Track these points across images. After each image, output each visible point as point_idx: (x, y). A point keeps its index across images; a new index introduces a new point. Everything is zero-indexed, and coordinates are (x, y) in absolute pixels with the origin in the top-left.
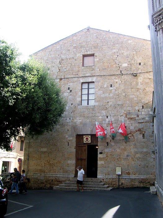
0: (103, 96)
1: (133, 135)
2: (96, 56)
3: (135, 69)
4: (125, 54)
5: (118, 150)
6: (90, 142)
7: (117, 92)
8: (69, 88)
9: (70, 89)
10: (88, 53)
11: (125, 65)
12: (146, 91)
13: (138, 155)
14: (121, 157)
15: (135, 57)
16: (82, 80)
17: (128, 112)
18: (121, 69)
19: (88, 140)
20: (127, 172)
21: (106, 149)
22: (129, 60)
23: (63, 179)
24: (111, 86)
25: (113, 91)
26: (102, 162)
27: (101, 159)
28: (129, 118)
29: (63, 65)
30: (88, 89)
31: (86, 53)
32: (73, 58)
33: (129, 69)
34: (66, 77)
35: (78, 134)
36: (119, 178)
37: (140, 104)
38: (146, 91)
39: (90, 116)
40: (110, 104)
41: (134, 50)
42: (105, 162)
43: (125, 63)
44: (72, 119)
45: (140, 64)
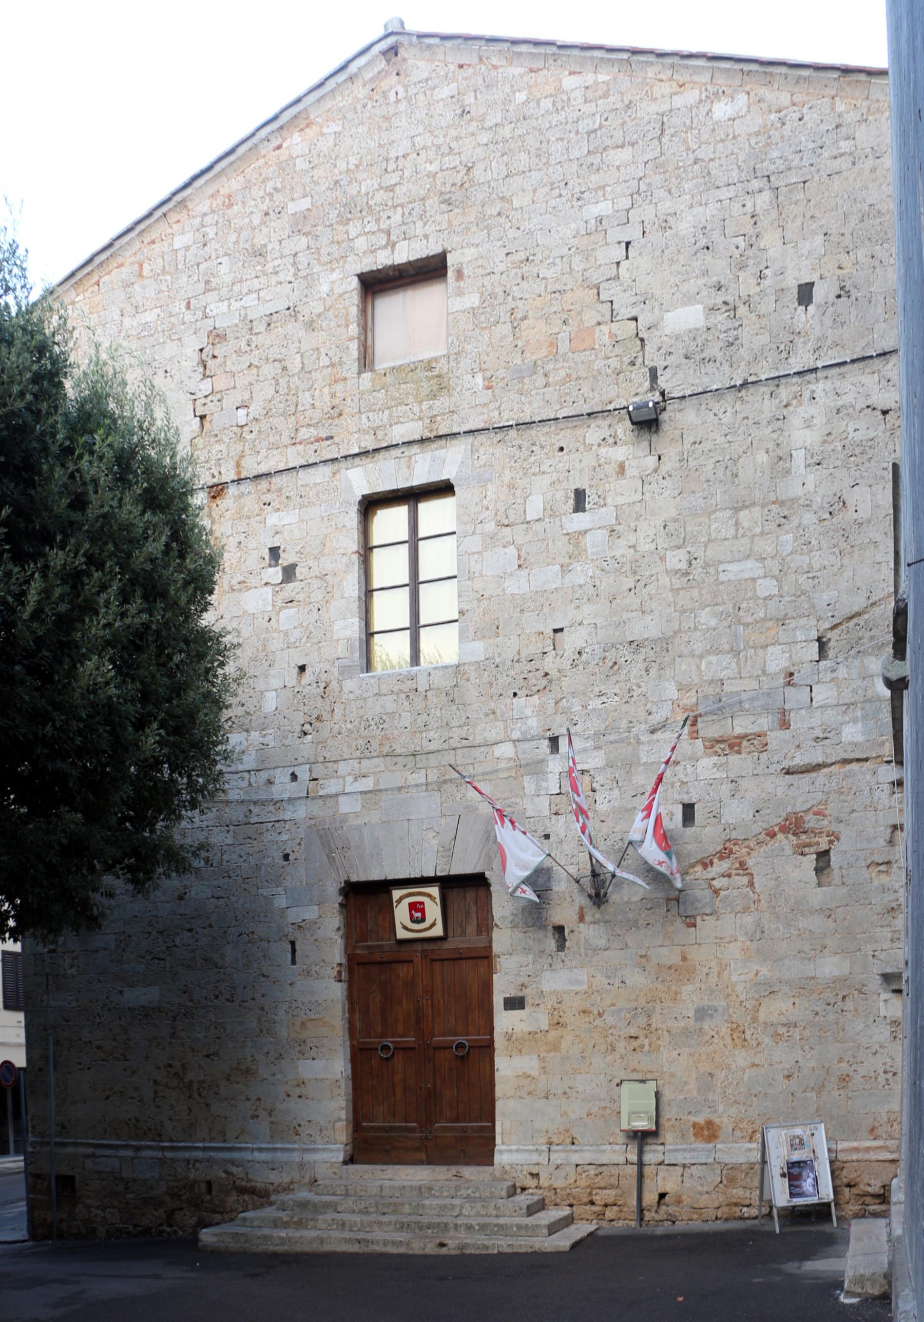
0: (517, 585)
1: (742, 865)
2: (460, 275)
3: (765, 338)
4: (685, 226)
5: (637, 979)
6: (438, 931)
7: (621, 549)
8: (274, 552)
9: (286, 559)
10: (403, 254)
11: (686, 317)
12: (850, 515)
13: (779, 1008)
14: (656, 1021)
15: (770, 239)
16: (363, 480)
17: (710, 690)
18: (653, 357)
19: (423, 919)
20: (695, 1125)
21: (547, 975)
22: (720, 269)
23: (274, 1177)
24: (580, 500)
25: (595, 541)
26: (528, 1063)
27: (517, 1044)
28: (719, 742)
29: (221, 382)
30: (414, 541)
31: (383, 259)
32: (292, 311)
33: (714, 351)
34: (251, 467)
35: (354, 878)
36: (641, 1164)
37: (803, 622)
38: (850, 515)
39: (432, 747)
40: (572, 641)
41: (756, 184)
42: (542, 1060)
43: (689, 299)
44: (307, 776)
45: (805, 294)
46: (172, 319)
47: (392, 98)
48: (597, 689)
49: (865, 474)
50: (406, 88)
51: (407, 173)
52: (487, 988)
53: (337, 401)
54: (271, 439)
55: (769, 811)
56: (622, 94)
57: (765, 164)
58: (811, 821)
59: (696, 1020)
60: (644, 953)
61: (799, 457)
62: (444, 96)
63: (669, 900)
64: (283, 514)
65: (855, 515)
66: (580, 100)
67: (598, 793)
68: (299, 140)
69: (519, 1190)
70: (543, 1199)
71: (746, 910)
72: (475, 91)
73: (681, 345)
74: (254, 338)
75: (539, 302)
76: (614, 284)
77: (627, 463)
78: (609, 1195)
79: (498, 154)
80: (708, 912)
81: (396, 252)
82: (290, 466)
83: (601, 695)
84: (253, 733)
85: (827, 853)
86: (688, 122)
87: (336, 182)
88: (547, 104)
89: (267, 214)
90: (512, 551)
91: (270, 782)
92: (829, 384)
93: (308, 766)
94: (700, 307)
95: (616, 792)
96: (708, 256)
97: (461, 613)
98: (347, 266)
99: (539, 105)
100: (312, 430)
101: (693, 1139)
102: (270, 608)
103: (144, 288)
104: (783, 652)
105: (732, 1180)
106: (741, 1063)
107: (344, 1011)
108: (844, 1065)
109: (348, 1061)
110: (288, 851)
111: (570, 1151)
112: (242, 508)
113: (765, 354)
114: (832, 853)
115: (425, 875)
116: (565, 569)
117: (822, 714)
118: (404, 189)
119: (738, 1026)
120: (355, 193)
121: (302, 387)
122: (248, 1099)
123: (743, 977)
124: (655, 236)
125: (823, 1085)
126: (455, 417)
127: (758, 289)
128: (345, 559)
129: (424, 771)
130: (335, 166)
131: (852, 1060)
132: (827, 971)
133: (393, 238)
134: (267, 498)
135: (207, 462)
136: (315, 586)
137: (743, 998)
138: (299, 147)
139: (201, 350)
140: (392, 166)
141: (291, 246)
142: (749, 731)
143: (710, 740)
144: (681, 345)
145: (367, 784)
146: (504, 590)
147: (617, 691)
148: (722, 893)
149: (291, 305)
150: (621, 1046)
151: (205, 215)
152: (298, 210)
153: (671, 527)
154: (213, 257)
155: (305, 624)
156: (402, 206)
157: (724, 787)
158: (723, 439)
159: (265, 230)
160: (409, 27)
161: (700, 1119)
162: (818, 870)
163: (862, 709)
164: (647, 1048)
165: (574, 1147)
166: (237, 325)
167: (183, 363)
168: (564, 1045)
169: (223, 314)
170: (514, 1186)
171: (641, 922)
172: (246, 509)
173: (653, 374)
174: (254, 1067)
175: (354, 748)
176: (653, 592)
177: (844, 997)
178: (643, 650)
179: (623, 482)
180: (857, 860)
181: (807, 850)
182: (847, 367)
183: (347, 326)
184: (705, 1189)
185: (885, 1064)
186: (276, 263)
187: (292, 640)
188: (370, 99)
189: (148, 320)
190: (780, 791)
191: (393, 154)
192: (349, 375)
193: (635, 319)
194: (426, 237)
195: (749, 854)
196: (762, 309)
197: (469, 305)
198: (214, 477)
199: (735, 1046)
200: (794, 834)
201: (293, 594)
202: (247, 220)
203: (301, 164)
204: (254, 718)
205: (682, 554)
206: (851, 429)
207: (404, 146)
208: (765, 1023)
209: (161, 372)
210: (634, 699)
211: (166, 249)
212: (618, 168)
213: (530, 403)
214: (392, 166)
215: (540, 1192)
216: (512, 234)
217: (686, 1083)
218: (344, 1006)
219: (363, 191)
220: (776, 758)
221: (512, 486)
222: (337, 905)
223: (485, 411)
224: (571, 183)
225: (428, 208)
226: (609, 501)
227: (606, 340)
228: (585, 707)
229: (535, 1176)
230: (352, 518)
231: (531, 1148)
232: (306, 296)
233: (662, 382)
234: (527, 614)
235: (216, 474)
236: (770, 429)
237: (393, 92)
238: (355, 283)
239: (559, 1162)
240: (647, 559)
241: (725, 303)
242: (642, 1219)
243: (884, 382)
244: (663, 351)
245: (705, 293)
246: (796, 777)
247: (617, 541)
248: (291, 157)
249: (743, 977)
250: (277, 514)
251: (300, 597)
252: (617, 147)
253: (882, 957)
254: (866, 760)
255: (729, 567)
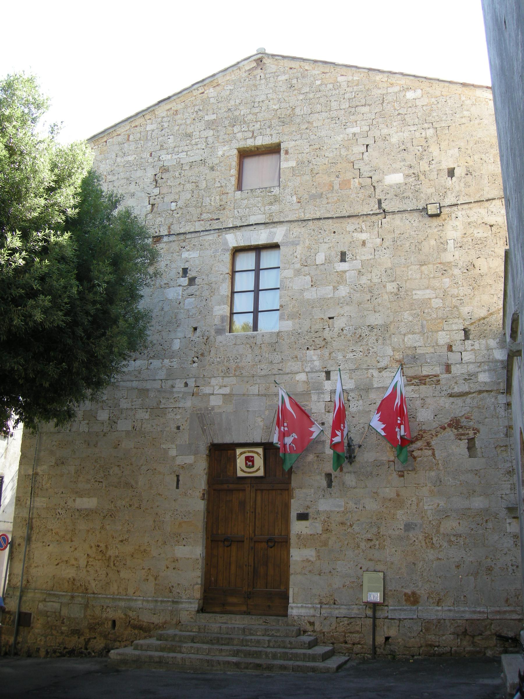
0: (311, 295)
1: (428, 444)
2: (287, 152)
3: (433, 190)
4: (394, 140)
5: (372, 505)
6: (261, 473)
7: (364, 280)
8: (185, 271)
9: (191, 274)
10: (260, 141)
11: (396, 178)
12: (477, 271)
13: (450, 525)
14: (383, 530)
15: (434, 150)
16: (233, 240)
17: (409, 352)
18: (379, 194)
19: (253, 466)
20: (405, 594)
21: (322, 501)
22: (410, 158)
24: (343, 257)
25: (350, 276)
26: (309, 553)
27: (305, 541)
28: (414, 378)
29: (164, 190)
30: (257, 270)
31: (250, 143)
32: (203, 162)
33: (408, 194)
34: (176, 229)
35: (216, 442)
36: (374, 618)
37: (456, 320)
38: (477, 271)
39: (263, 373)
40: (339, 323)
41: (426, 126)
42: (318, 551)
43: (395, 171)
44: (193, 385)
45: (451, 173)
46: (142, 160)
47: (258, 78)
48: (351, 348)
49: (483, 253)
50: (265, 74)
51: (263, 109)
52: (287, 507)
53: (223, 203)
54: (188, 217)
55: (441, 416)
56: (365, 85)
57: (430, 118)
58: (464, 422)
59: (405, 531)
60: (375, 491)
61: (451, 243)
62: (283, 79)
63: (389, 461)
64: (191, 253)
65: (480, 272)
66: (346, 86)
67: (351, 402)
68: (213, 91)
69: (302, 632)
70: (317, 639)
71: (431, 469)
72: (297, 79)
73: (393, 190)
74: (183, 172)
75: (324, 167)
76: (361, 161)
77: (367, 241)
78: (356, 637)
79: (307, 104)
80: (410, 469)
81: (256, 140)
82: (197, 230)
83: (353, 351)
84: (165, 360)
85: (473, 439)
86: (395, 99)
87: (229, 109)
88: (330, 86)
89: (194, 119)
90: (308, 278)
91: (173, 387)
92: (464, 212)
93: (194, 379)
94: (401, 174)
95: (361, 401)
96: (405, 154)
97: (281, 306)
98: (232, 145)
99: (326, 87)
100: (209, 215)
101: (404, 603)
102: (180, 297)
103: (129, 146)
104: (447, 335)
105: (427, 630)
106: (431, 557)
107: (204, 517)
108: (489, 560)
109: (204, 548)
110: (179, 424)
111: (334, 608)
112: (169, 249)
113: (433, 197)
114: (476, 440)
115: (255, 441)
116: (335, 288)
117: (467, 366)
118: (262, 115)
119: (429, 535)
120: (238, 114)
121: (205, 195)
122: (143, 569)
123: (430, 507)
124: (380, 143)
125: (478, 572)
126: (282, 214)
127: (429, 169)
128: (222, 276)
129: (257, 385)
130: (229, 103)
131: (493, 557)
132: (477, 505)
133: (255, 134)
134: (184, 244)
135: (153, 225)
136: (205, 289)
137: (431, 519)
138: (212, 94)
139: (155, 175)
140: (256, 105)
141: (204, 134)
142: (430, 374)
143: (409, 377)
144: (393, 190)
145: (227, 391)
146: (303, 297)
147: (362, 350)
148: (419, 459)
149: (203, 159)
150: (363, 545)
151: (163, 117)
152: (210, 119)
153: (389, 271)
154: (166, 135)
155: (198, 306)
156: (260, 122)
157: (417, 402)
158: (414, 233)
159: (193, 126)
160: (267, 52)
161: (408, 591)
162: (469, 448)
163: (488, 365)
164: (377, 546)
165: (335, 606)
166: (175, 165)
167: (146, 180)
168: (330, 543)
169: (167, 159)
170: (300, 629)
171: (374, 473)
172: (172, 249)
173: (380, 202)
174: (148, 549)
175: (220, 371)
176: (380, 302)
177: (486, 521)
178: (375, 330)
179: (365, 249)
180: (489, 444)
181: (463, 437)
182: (472, 204)
183: (230, 170)
184: (412, 635)
185: (511, 560)
186: (197, 140)
187: (191, 314)
188: (248, 77)
189: (130, 159)
190: (447, 406)
191: (257, 100)
192: (229, 192)
193: (371, 178)
194: (271, 135)
195: (432, 438)
196: (432, 178)
197: (291, 165)
198: (156, 233)
199: (427, 547)
200: (455, 429)
201: (193, 291)
202: (184, 121)
203: (212, 100)
204: (167, 352)
205: (394, 285)
206: (475, 232)
207: (263, 97)
208: (443, 534)
209: (134, 183)
210: (370, 354)
211: (142, 130)
212: (363, 114)
213: (320, 211)
214: (256, 105)
215: (315, 634)
216: (312, 137)
217: (400, 569)
218: (204, 514)
219: (242, 114)
220: (444, 388)
221: (309, 248)
222: (205, 456)
223: (297, 212)
224: (341, 118)
225: (273, 123)
226: (358, 257)
227: (357, 185)
228: (344, 357)
229: (312, 624)
230: (227, 257)
231: (310, 605)
232: (211, 156)
233: (383, 205)
234: (315, 309)
235: (158, 231)
236: (436, 230)
237: (259, 76)
238: (236, 152)
239: (326, 615)
240: (377, 286)
241: (414, 174)
242: (375, 653)
243: (490, 213)
244: (384, 192)
245: (404, 168)
246: (455, 399)
247: (362, 277)
248: (208, 97)
249: (430, 507)
250: (188, 253)
251: (197, 293)
252: (362, 106)
253: (505, 498)
254: (491, 391)
255: (418, 292)
